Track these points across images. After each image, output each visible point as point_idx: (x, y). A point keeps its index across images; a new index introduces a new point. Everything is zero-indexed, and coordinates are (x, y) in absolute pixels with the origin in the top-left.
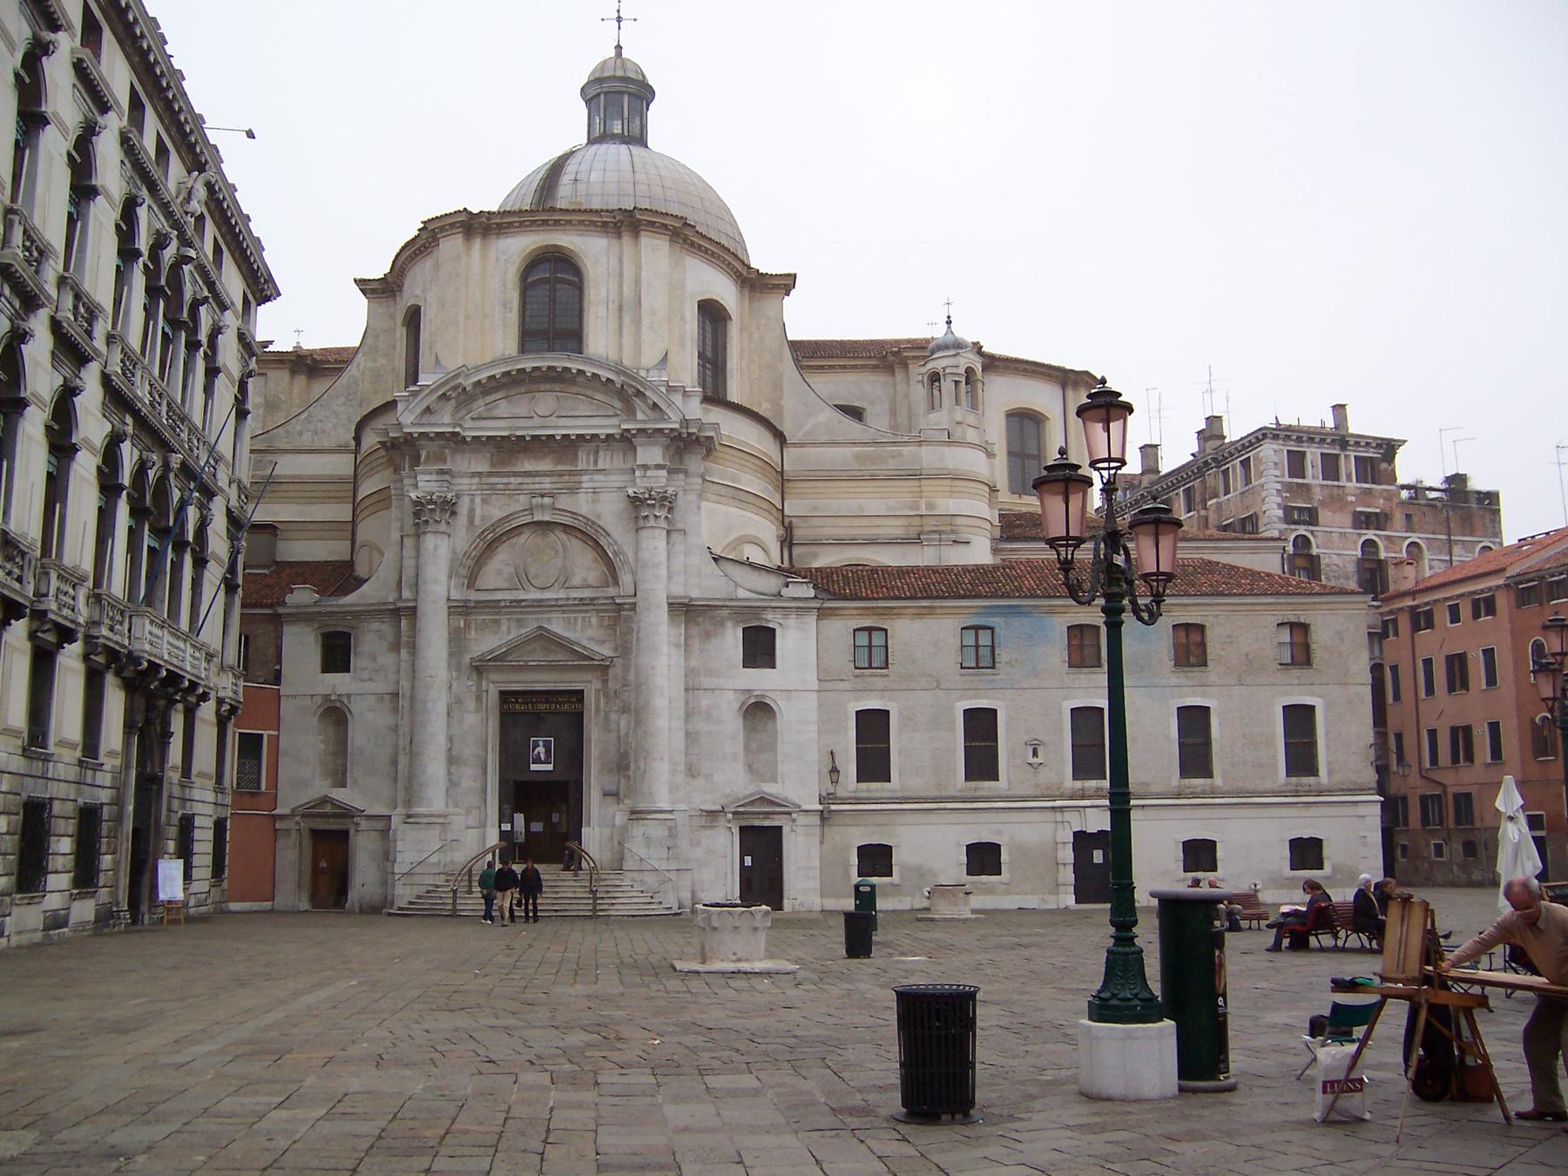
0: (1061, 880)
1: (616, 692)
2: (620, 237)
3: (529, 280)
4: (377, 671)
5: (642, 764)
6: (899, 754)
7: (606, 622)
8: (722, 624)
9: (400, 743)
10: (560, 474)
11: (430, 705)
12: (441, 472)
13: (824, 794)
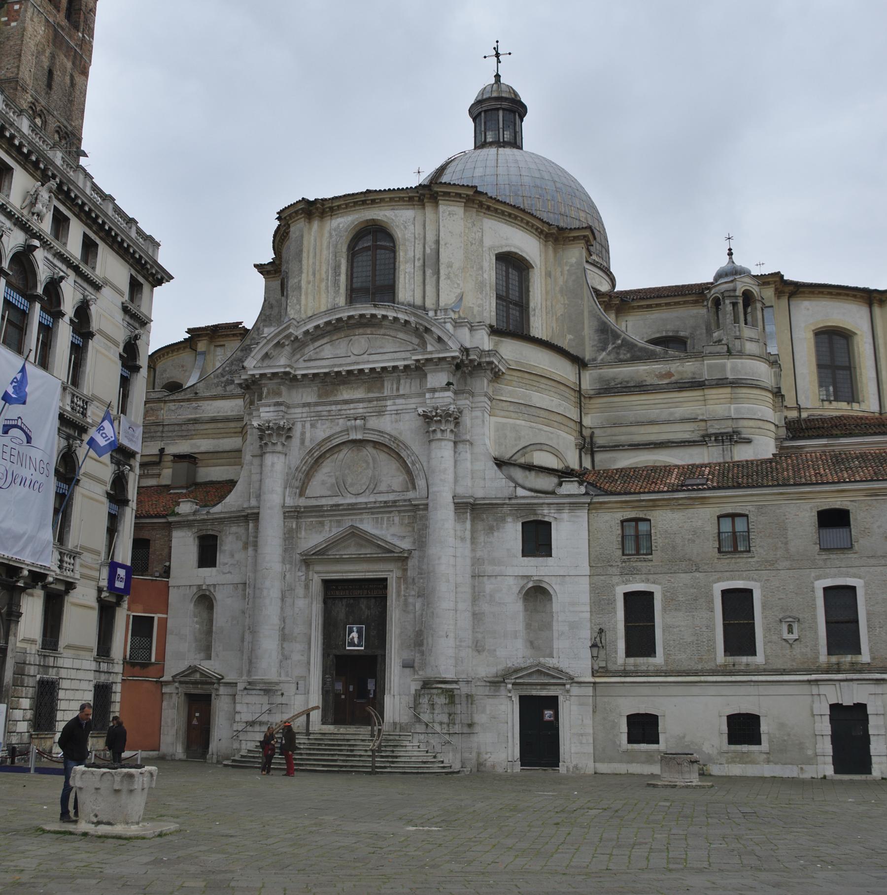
0: (819, 751)
1: (414, 579)
2: (423, 206)
3: (357, 249)
4: (234, 565)
5: (430, 640)
6: (664, 631)
7: (406, 522)
8: (503, 520)
9: (246, 624)
10: (370, 400)
11: (265, 593)
12: (277, 404)
13: (596, 667)
